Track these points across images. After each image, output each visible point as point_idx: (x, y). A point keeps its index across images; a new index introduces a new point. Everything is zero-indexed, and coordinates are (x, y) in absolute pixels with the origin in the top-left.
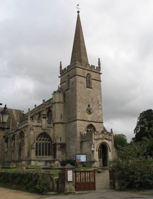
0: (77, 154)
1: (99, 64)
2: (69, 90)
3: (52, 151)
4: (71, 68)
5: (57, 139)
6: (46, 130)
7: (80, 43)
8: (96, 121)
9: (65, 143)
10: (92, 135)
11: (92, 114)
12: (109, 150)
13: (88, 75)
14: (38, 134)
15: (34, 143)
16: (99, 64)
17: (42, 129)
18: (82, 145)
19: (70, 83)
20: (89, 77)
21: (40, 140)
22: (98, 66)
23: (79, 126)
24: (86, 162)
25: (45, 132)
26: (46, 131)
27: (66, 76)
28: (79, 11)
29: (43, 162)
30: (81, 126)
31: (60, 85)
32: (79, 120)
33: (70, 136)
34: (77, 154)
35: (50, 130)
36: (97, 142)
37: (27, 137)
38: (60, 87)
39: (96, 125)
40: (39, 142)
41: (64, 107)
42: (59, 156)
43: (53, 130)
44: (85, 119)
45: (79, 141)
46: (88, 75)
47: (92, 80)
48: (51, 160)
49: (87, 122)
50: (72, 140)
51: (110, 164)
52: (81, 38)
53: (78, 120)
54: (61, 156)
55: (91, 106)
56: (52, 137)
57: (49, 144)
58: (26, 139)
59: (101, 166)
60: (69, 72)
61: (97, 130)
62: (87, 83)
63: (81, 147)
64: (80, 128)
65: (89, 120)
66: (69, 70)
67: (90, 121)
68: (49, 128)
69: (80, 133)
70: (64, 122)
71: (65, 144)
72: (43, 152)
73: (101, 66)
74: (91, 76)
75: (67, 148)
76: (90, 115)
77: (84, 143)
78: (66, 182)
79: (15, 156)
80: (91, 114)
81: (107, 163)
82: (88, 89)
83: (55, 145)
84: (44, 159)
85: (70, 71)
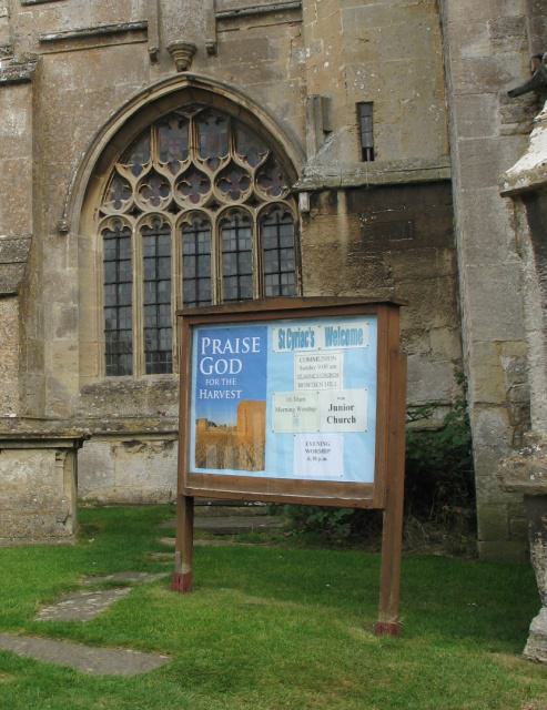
17: (154, 58)
25: (195, 88)
26: (209, 72)
35: (263, 48)
68: (244, 27)
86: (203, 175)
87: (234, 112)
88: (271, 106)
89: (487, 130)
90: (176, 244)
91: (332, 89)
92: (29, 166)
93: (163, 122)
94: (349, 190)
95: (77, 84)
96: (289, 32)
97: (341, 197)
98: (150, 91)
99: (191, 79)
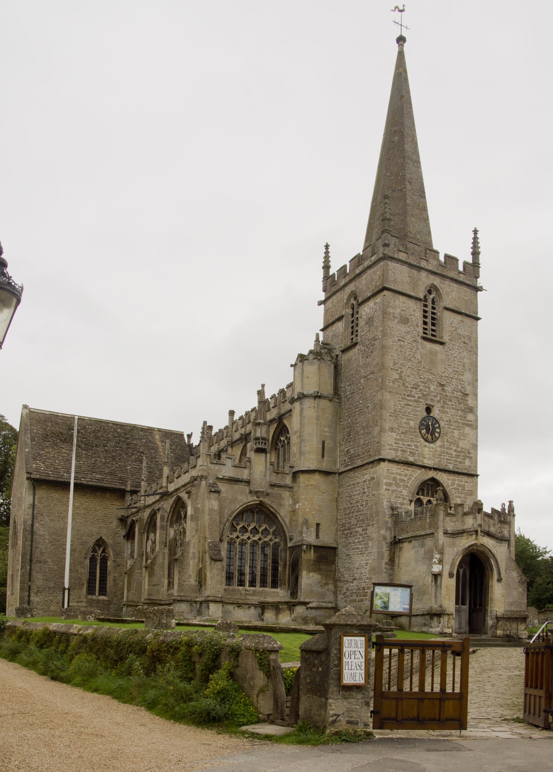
0: (375, 584)
1: (475, 253)
2: (357, 347)
3: (284, 572)
4: (367, 263)
5: (305, 529)
6: (268, 494)
7: (403, 167)
8: (451, 467)
9: (335, 546)
10: (434, 515)
11: (438, 443)
12: (495, 576)
13: (430, 292)
14: (237, 507)
15: (221, 540)
16: (475, 253)
17: (251, 492)
18: (397, 553)
19: (362, 323)
20: (433, 302)
21: (244, 529)
22: (470, 260)
23: (390, 484)
24: (410, 615)
26: (266, 500)
27: (346, 297)
28: (404, 35)
29: (252, 608)
30: (397, 485)
31: (321, 334)
32: (390, 461)
33: (353, 521)
34: (375, 584)
35: (280, 497)
36: (454, 545)
37: (195, 518)
38: (321, 339)
39: (453, 484)
40: (238, 537)
41: (338, 416)
42: (311, 591)
43: (293, 497)
44: (411, 459)
45: (385, 538)
46: (430, 292)
47: (447, 313)
48: (279, 602)
49: (419, 471)
50: (361, 535)
51: (495, 627)
52: (406, 147)
53: (383, 460)
54: (318, 589)
55: (435, 413)
56: (288, 524)
57: (276, 547)
58: (189, 525)
59: (462, 630)
60: (357, 283)
61: (455, 499)
62: (425, 323)
63: (392, 561)
64: (393, 491)
65: (427, 462)
66: (358, 271)
67: (430, 468)
68: (276, 489)
69: (392, 509)
70: (333, 469)
71: (335, 549)
72: (253, 574)
73: (482, 259)
74: (439, 295)
75: (341, 563)
76: (432, 445)
77: (406, 546)
78: (333, 688)
79: (154, 585)
80: (433, 441)
81: (484, 621)
82: (429, 345)
83: (297, 549)
84: (255, 599)
85: (359, 275)
86: (258, 530)
87: (268, 512)
88: (281, 514)
89: (383, 549)
90: (247, 549)
91: (310, 517)
92: (218, 520)
93: (247, 511)
94: (315, 546)
95: (227, 494)
96: (288, 493)
97: (312, 547)
98: (249, 502)
99: (261, 501)
